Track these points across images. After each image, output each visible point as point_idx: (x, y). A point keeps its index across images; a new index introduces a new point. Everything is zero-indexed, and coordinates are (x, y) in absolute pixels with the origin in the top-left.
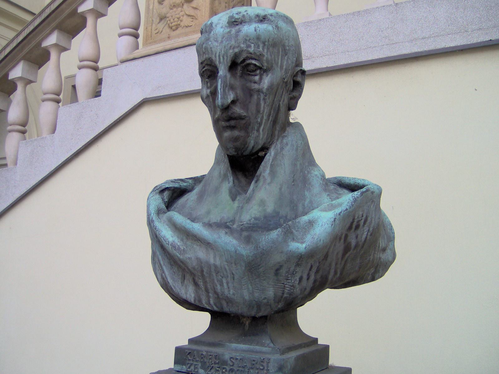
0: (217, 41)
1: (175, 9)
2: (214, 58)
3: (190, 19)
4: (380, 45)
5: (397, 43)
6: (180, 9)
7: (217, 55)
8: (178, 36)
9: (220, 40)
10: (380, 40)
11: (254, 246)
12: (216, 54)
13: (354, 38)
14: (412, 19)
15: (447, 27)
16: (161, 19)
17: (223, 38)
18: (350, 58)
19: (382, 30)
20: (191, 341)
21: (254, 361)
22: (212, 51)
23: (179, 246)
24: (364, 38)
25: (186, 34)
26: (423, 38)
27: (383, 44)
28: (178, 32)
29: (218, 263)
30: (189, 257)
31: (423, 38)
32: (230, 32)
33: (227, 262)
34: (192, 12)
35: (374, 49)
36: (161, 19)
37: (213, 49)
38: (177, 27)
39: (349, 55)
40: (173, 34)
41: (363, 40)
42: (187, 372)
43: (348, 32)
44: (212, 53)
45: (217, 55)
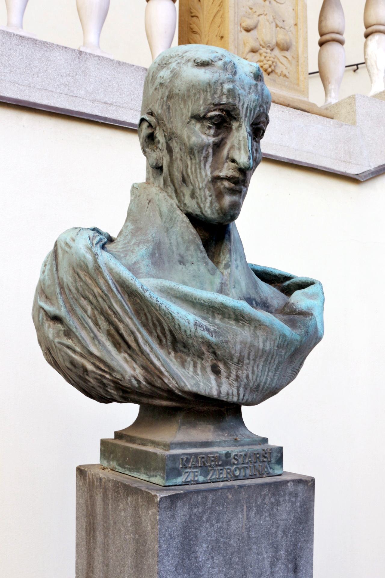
0: (243, 88)
2: (240, 108)
4: (58, 91)
5: (77, 97)
7: (245, 106)
9: (247, 89)
10: (58, 85)
11: (303, 331)
12: (243, 104)
13: (27, 70)
14: (96, 77)
15: (130, 100)
17: (250, 88)
18: (20, 93)
19: (62, 75)
21: (258, 454)
22: (239, 98)
23: (206, 326)
24: (40, 75)
26: (105, 103)
27: (61, 92)
29: (268, 347)
30: (226, 341)
31: (105, 103)
32: (256, 85)
33: (278, 346)
35: (51, 93)
37: (241, 97)
39: (19, 88)
41: (38, 77)
42: (184, 483)
43: (20, 59)
44: (239, 101)
45: (245, 106)
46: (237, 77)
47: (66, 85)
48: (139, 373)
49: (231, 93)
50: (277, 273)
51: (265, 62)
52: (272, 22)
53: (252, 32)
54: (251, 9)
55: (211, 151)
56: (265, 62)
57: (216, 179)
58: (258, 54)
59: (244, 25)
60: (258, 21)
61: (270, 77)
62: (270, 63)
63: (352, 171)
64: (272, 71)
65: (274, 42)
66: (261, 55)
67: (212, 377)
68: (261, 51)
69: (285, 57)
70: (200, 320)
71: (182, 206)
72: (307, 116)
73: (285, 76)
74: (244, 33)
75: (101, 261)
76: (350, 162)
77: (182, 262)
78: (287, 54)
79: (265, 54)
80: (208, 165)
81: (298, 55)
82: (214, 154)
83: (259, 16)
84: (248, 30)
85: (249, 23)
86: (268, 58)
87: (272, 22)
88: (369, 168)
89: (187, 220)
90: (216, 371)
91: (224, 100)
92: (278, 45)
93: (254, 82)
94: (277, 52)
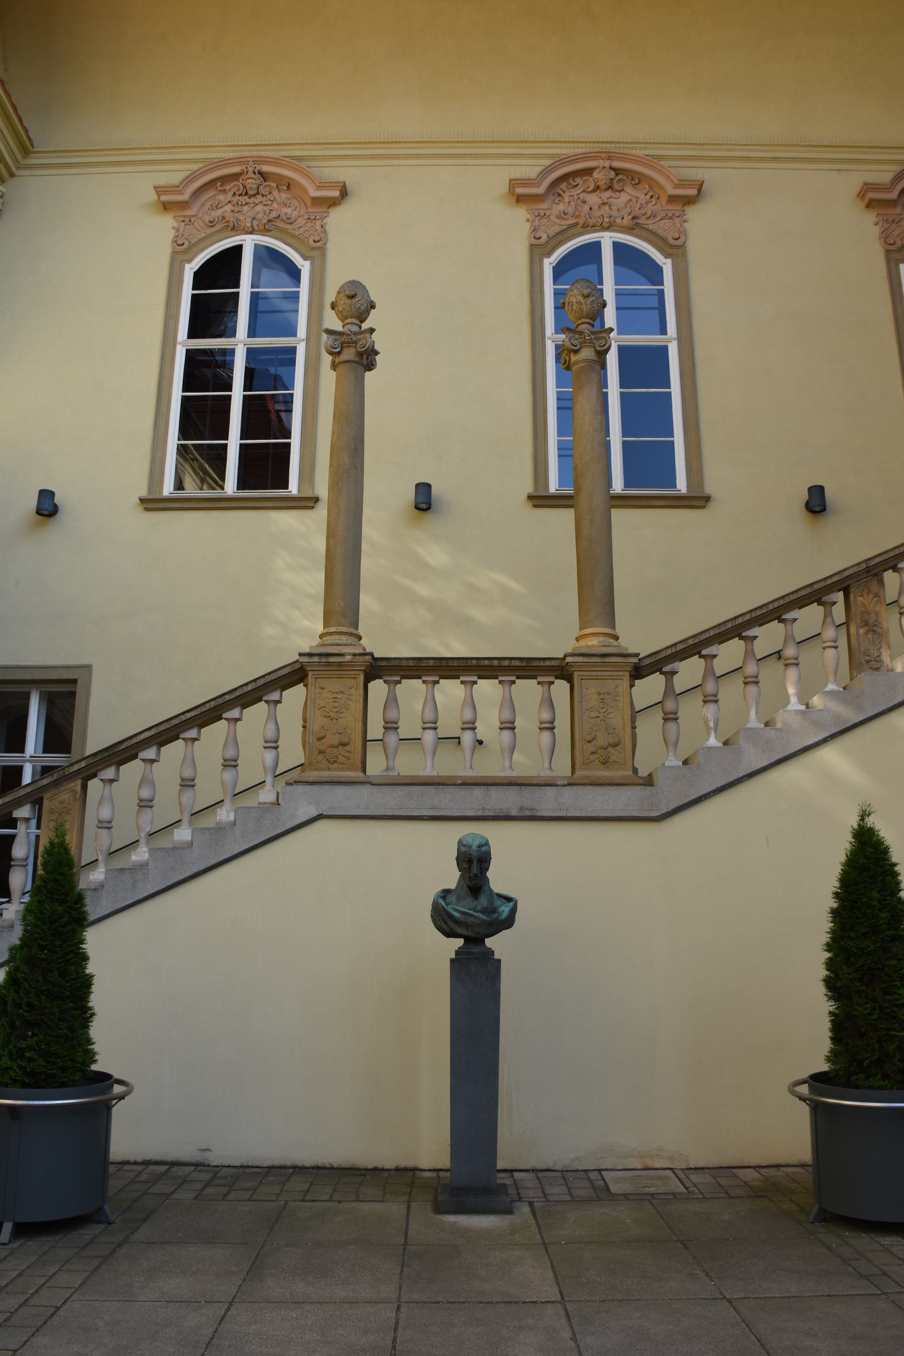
0: (473, 852)
1: (332, 749)
3: (344, 759)
6: (336, 749)
8: (336, 770)
16: (320, 753)
20: (459, 948)
25: (343, 770)
28: (335, 765)
34: (346, 754)
36: (320, 753)
38: (335, 762)
40: (331, 766)
46: (471, 849)
47: (481, 805)
48: (449, 929)
49: (470, 854)
50: (509, 897)
51: (601, 758)
52: (605, 733)
53: (592, 743)
54: (591, 728)
55: (468, 869)
56: (601, 758)
57: (470, 877)
58: (597, 754)
59: (586, 740)
60: (596, 735)
61: (606, 765)
62: (604, 758)
63: (655, 814)
64: (606, 762)
65: (607, 744)
66: (598, 754)
67: (466, 931)
68: (598, 752)
69: (616, 750)
70: (460, 916)
71: (466, 883)
72: (620, 789)
73: (616, 762)
74: (587, 744)
75: (439, 901)
76: (652, 810)
77: (464, 899)
78: (617, 748)
79: (600, 754)
80: (468, 873)
81: (625, 747)
82: (469, 870)
83: (597, 731)
84: (589, 742)
85: (589, 738)
86: (602, 755)
87: (605, 733)
88: (667, 811)
89: (466, 887)
90: (467, 929)
91: (468, 856)
92: (609, 745)
93: (477, 849)
94: (610, 749)
